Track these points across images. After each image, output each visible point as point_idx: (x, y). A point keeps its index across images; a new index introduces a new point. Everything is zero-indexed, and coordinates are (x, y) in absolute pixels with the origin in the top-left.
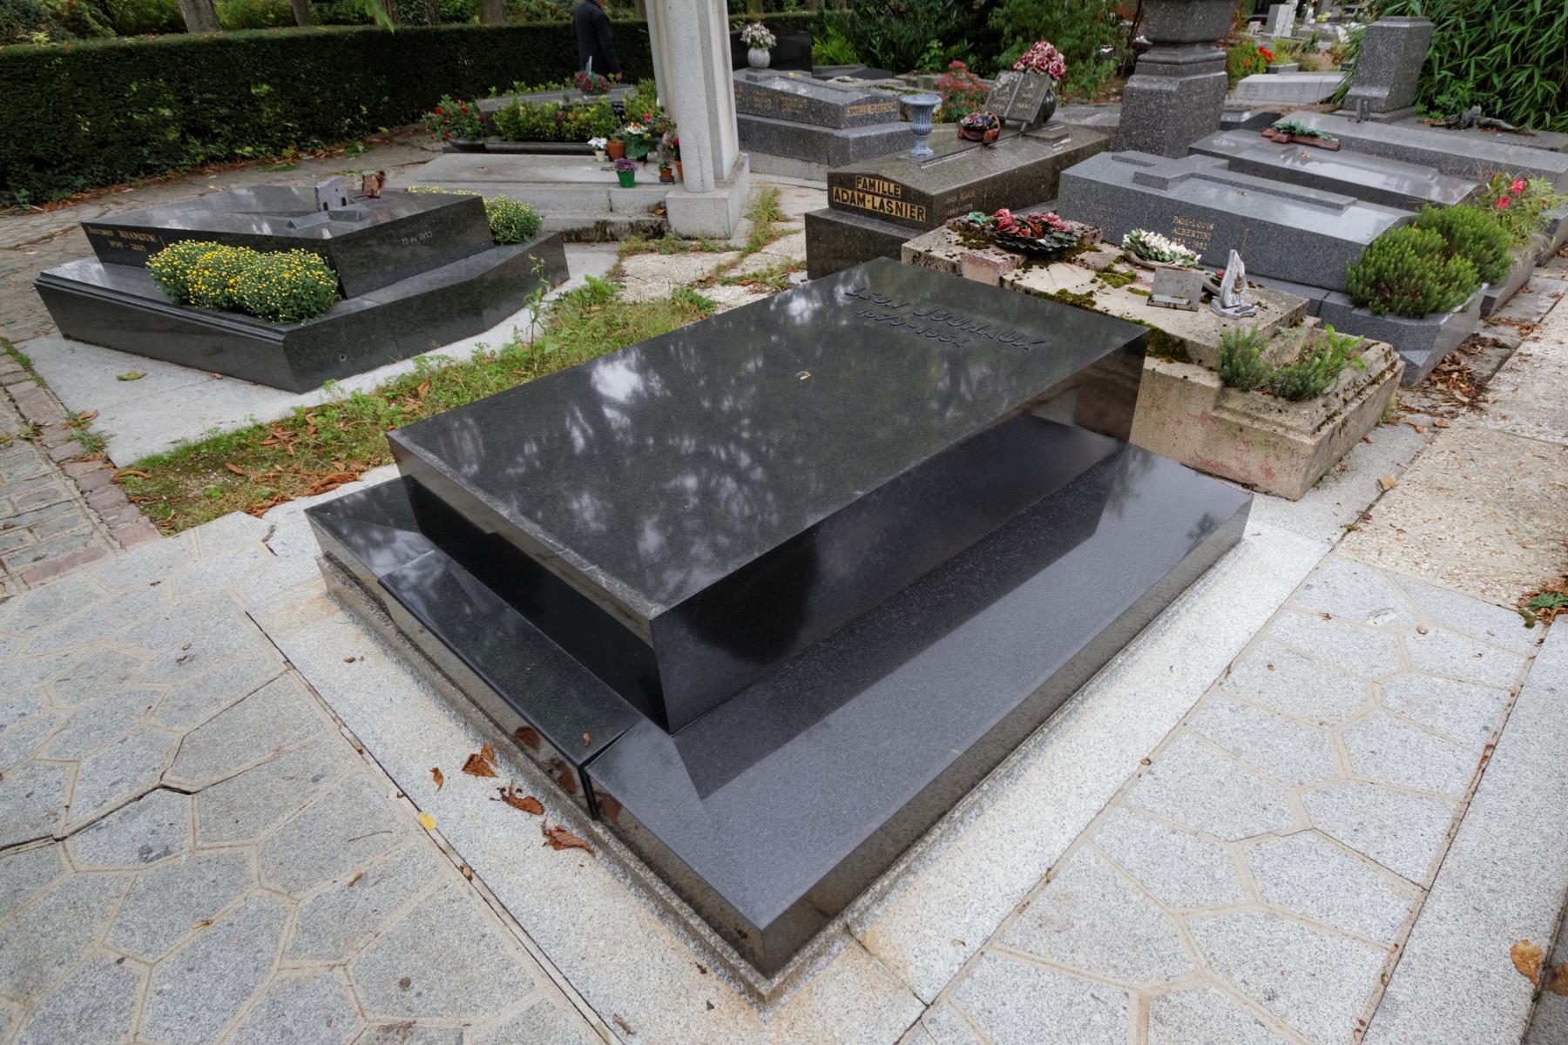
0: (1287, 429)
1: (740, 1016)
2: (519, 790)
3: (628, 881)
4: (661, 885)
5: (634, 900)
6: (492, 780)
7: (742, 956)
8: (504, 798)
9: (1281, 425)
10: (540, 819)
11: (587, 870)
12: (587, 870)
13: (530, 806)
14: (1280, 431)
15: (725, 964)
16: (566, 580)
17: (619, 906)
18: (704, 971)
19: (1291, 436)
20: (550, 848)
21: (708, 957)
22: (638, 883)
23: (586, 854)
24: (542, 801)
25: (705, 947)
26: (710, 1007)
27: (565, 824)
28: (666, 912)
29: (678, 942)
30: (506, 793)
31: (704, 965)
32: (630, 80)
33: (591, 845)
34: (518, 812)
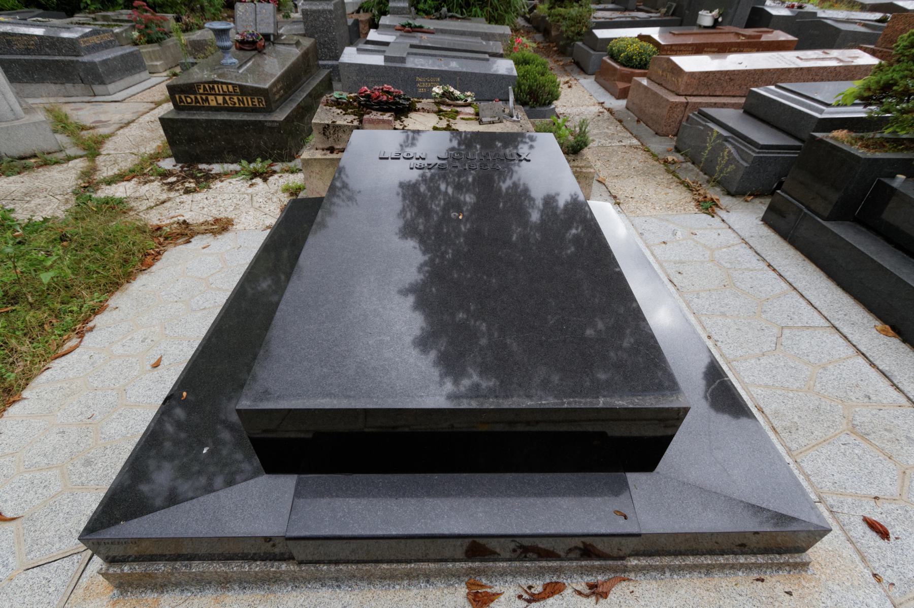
0: (580, 168)
1: (804, 583)
2: (530, 587)
3: (668, 574)
4: (703, 558)
5: (683, 581)
6: (502, 598)
7: (780, 553)
8: (529, 601)
9: (577, 167)
10: (568, 591)
11: (638, 591)
12: (638, 591)
13: (553, 589)
14: (578, 169)
15: (770, 566)
16: (270, 435)
17: (683, 592)
18: (763, 580)
19: (584, 170)
20: (601, 601)
21: (755, 571)
22: (674, 570)
23: (624, 584)
24: (555, 579)
25: (748, 567)
26: (790, 593)
27: (591, 579)
28: (709, 570)
29: (732, 579)
30: (526, 596)
31: (756, 576)
32: (307, 10)
33: (622, 574)
34: (550, 601)
